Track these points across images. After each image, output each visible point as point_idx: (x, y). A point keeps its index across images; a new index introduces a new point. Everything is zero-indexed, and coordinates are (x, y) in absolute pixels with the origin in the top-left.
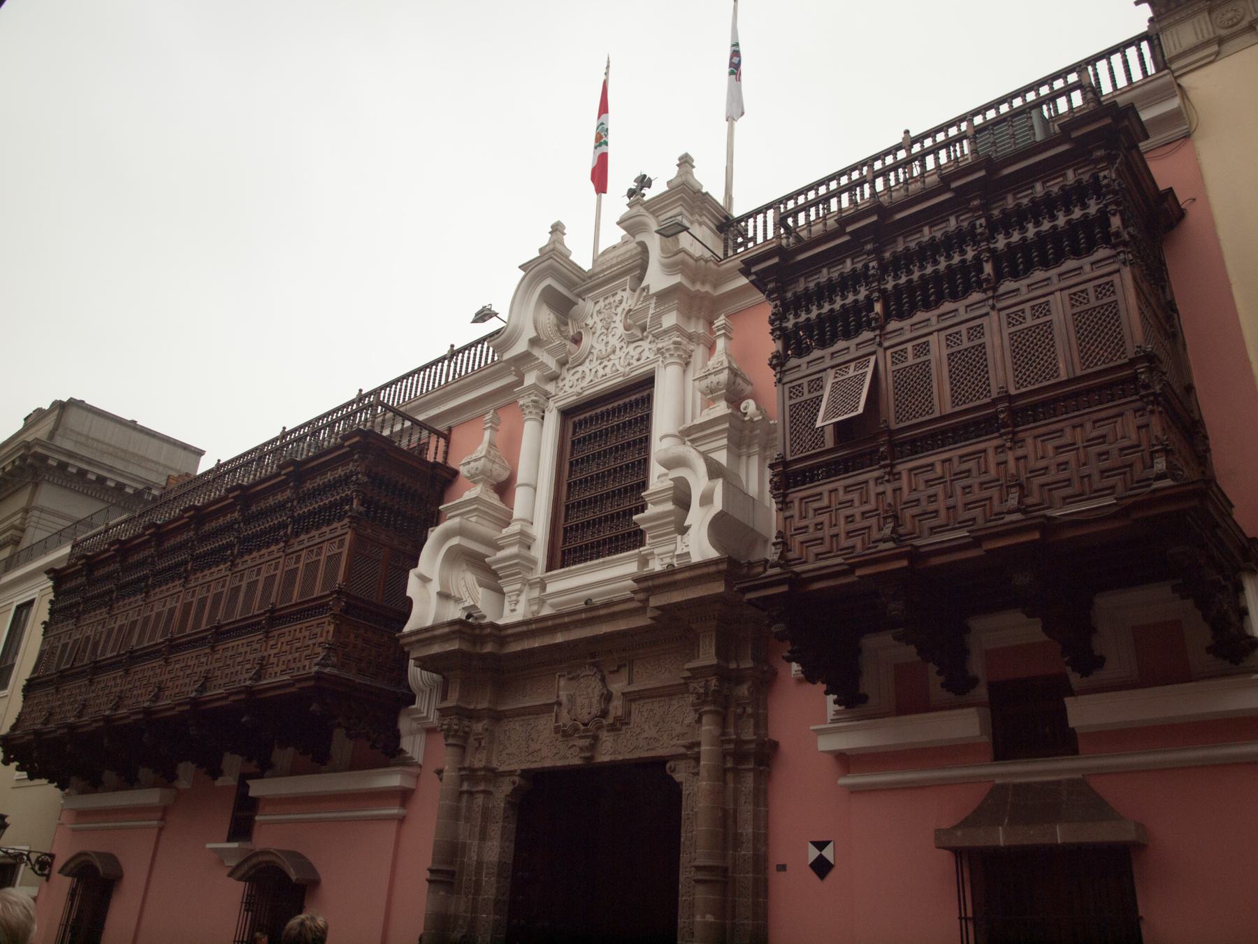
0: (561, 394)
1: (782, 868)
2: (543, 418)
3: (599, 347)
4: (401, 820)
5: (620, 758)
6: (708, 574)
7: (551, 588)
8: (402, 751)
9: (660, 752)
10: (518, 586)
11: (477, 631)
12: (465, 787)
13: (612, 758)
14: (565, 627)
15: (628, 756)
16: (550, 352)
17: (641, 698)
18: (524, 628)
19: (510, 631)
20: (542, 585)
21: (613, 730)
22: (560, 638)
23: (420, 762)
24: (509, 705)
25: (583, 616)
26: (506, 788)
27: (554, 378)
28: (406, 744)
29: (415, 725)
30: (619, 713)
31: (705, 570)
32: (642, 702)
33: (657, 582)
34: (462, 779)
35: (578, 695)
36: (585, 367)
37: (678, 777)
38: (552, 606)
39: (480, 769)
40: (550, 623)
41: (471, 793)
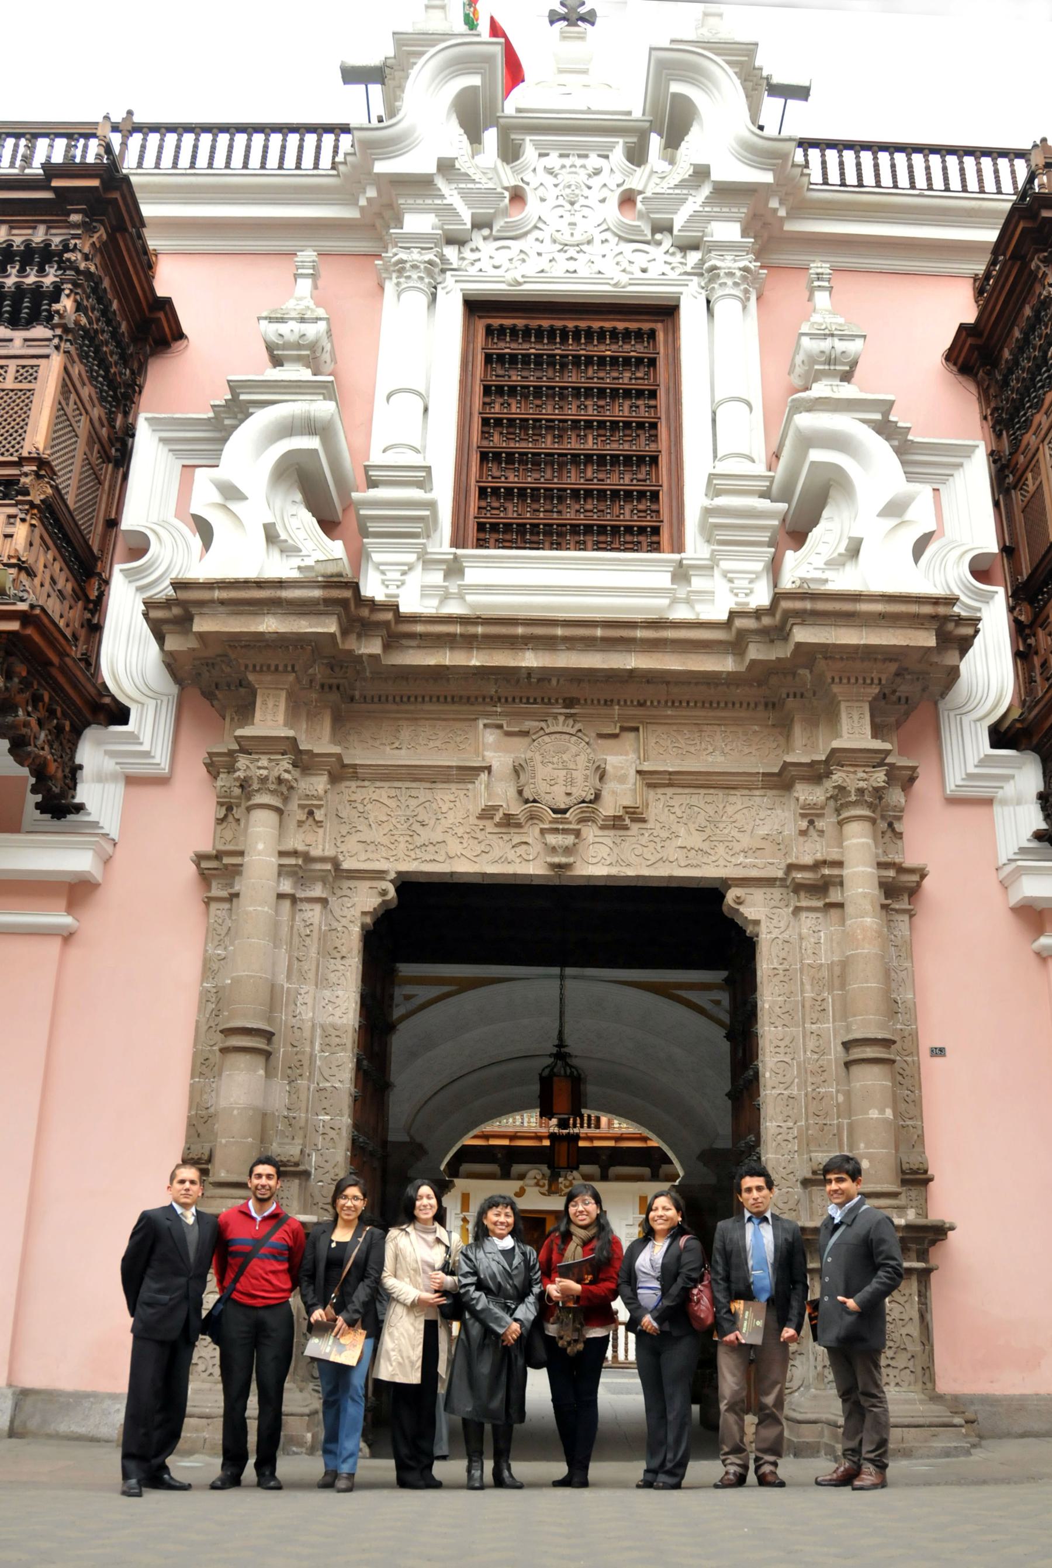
0: (473, 271)
1: (939, 1052)
2: (434, 296)
3: (555, 223)
4: (68, 937)
5: (631, 872)
6: (916, 616)
7: (473, 575)
8: (79, 808)
9: (709, 870)
10: (412, 558)
11: (365, 612)
12: (286, 886)
13: (614, 871)
14: (549, 643)
15: (646, 872)
16: (465, 195)
17: (670, 785)
18: (458, 629)
19: (419, 628)
20: (454, 569)
21: (614, 827)
22: (530, 660)
23: (114, 834)
24: (359, 755)
25: (599, 632)
26: (366, 900)
27: (457, 241)
28: (85, 793)
29: (110, 765)
30: (628, 802)
31: (914, 609)
32: (670, 791)
33: (821, 606)
34: (282, 871)
35: (562, 762)
36: (528, 243)
37: (749, 912)
38: (471, 606)
39: (323, 860)
40: (520, 630)
41: (294, 899)
